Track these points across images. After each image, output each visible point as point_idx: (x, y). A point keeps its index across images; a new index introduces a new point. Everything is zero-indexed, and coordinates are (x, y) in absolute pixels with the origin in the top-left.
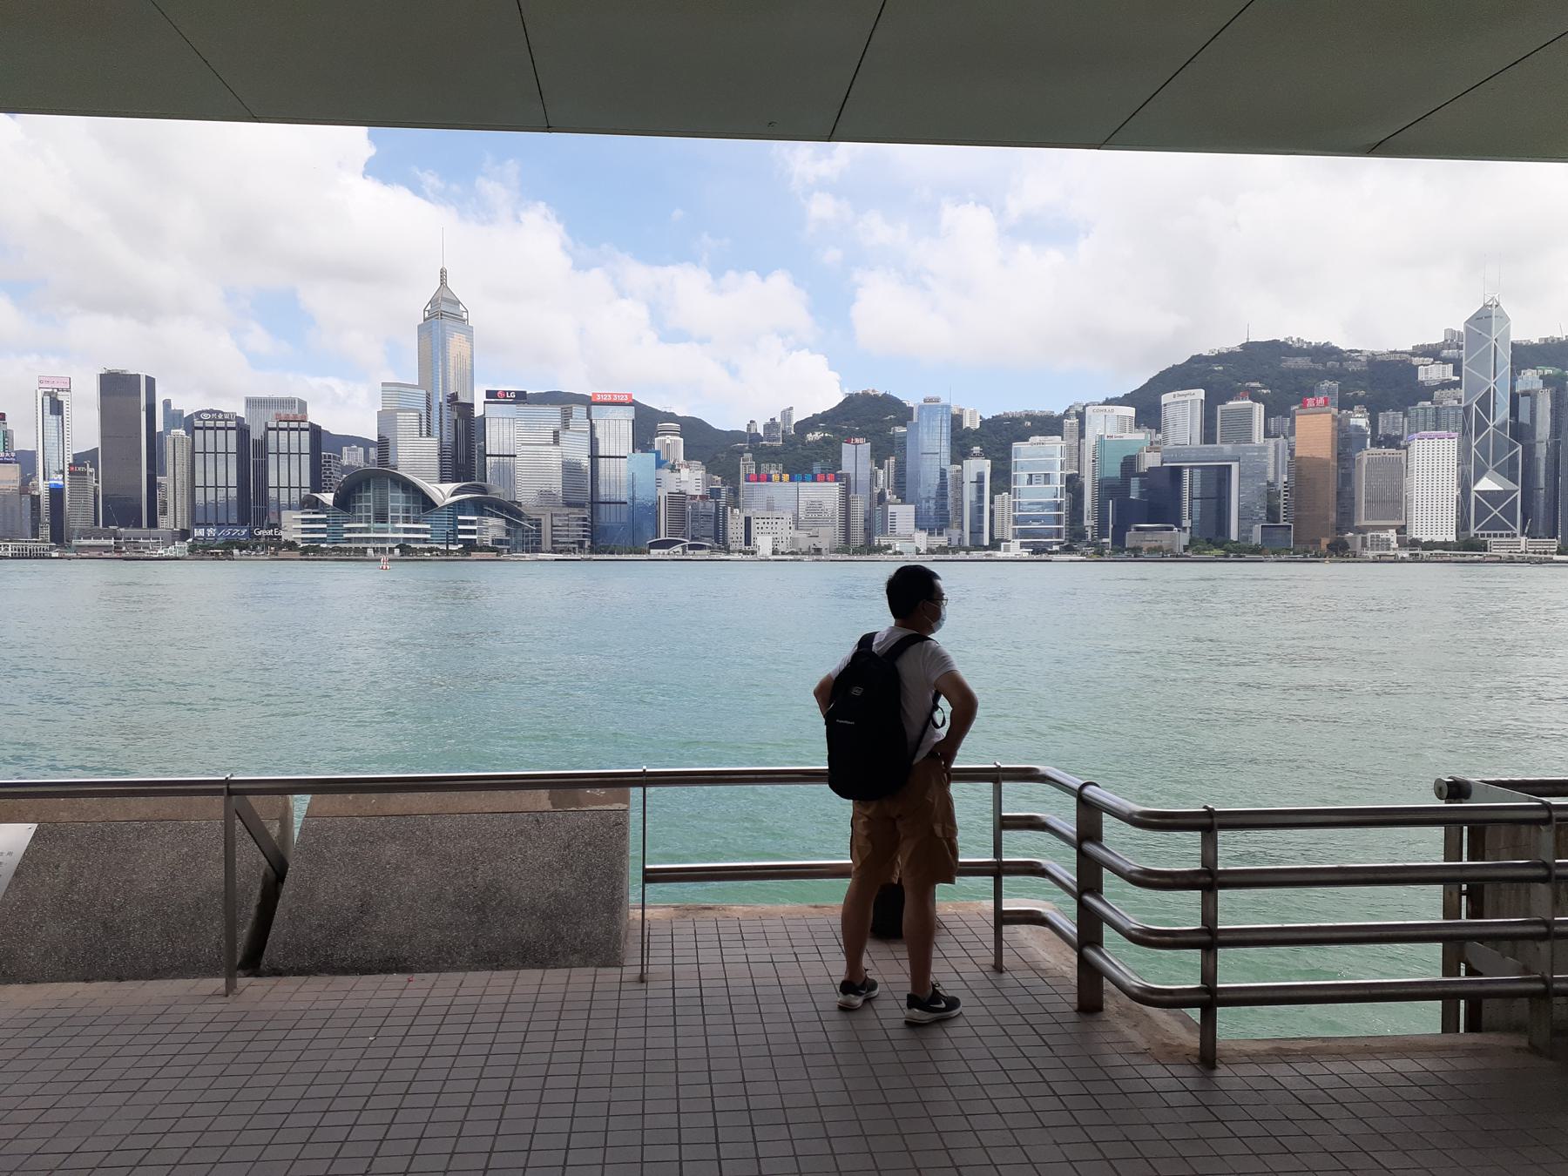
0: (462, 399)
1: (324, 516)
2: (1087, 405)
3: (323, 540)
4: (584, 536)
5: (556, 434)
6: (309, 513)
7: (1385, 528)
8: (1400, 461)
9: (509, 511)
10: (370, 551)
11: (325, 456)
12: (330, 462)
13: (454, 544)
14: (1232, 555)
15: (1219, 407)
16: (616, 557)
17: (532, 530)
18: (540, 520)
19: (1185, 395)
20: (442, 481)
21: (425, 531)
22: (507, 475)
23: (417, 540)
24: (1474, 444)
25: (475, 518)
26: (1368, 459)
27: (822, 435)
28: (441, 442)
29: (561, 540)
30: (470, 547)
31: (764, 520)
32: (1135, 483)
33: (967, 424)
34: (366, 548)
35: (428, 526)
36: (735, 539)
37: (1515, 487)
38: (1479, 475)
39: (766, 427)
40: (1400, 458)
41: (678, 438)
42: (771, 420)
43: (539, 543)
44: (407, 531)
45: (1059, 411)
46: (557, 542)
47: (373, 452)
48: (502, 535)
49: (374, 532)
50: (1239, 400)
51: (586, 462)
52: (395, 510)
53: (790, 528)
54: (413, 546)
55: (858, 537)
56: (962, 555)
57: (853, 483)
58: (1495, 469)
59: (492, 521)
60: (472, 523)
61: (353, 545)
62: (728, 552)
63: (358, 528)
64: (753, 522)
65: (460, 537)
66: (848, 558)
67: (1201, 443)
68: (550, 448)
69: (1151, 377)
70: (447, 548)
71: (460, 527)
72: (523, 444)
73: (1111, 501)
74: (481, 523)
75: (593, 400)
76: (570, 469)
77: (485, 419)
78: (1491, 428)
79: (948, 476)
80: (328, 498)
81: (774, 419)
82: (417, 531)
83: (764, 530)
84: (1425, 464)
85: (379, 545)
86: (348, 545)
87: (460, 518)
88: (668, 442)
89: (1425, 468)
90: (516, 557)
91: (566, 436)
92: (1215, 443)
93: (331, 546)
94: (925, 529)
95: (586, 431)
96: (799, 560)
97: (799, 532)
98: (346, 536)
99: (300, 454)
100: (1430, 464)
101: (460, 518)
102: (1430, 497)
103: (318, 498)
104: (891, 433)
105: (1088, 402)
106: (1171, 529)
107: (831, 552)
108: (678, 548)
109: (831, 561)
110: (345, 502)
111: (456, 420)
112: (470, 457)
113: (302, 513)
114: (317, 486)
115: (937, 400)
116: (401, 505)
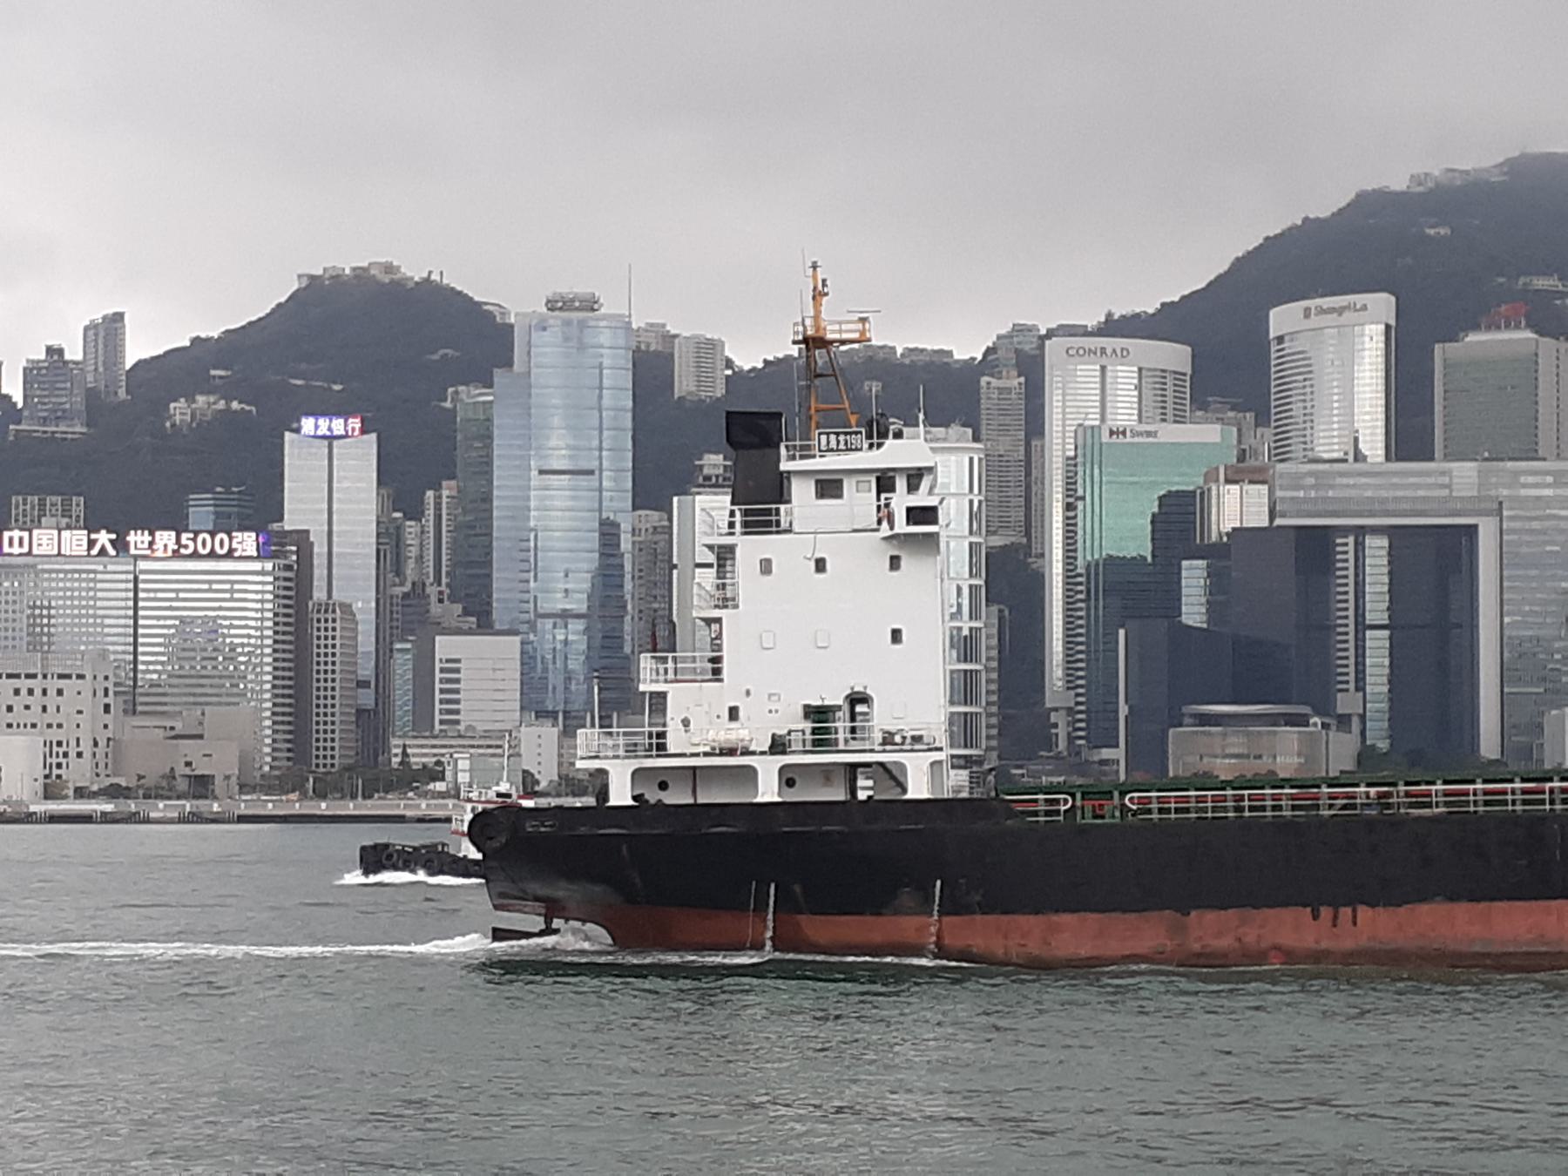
2: (1051, 334)
15: (1438, 347)
19: (1340, 311)
32: (1193, 575)
33: (684, 384)
39: (32, 374)
42: (50, 350)
45: (967, 348)
50: (1498, 328)
53: (107, 708)
57: (319, 562)
67: (1388, 458)
73: (1122, 632)
79: (626, 543)
92: (1431, 459)
94: (553, 715)
96: (132, 818)
104: (448, 405)
105: (1054, 326)
107: (243, 788)
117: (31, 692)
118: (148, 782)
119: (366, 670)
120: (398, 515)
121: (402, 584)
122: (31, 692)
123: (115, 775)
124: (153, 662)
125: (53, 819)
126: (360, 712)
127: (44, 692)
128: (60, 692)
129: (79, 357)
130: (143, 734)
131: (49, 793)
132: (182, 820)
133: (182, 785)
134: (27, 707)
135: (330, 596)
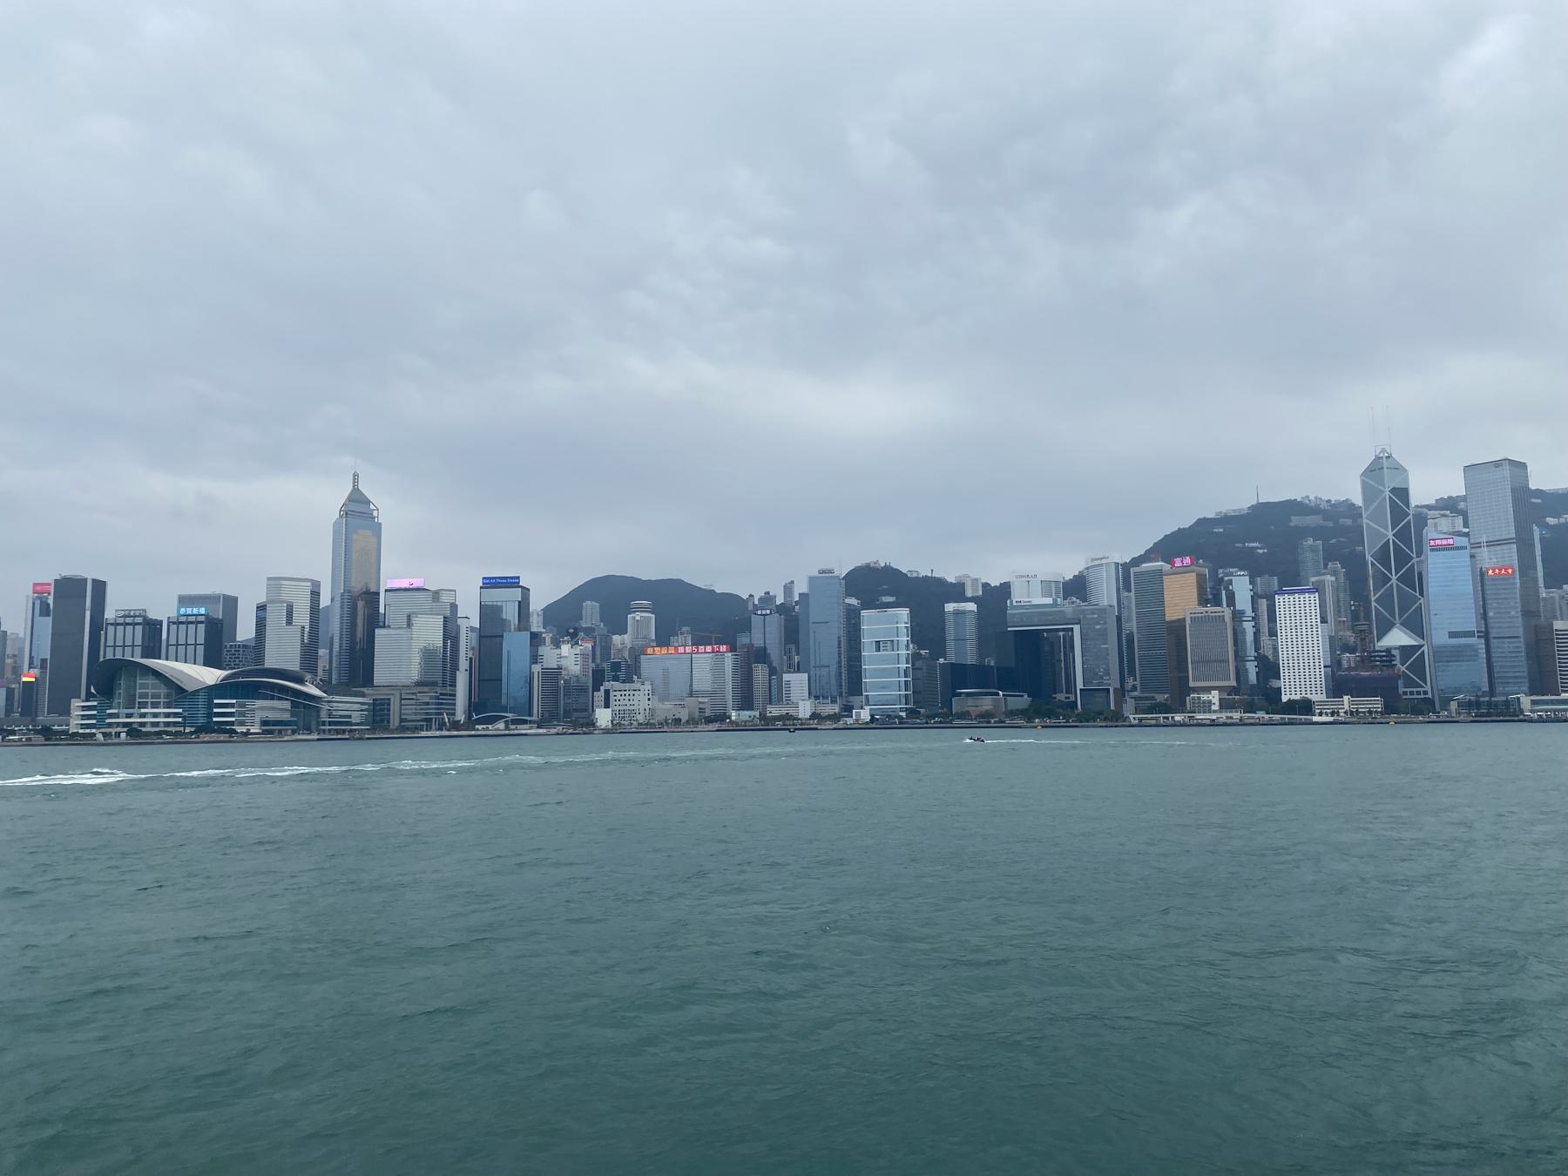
0: (373, 589)
7: (1208, 690)
8: (1224, 619)
10: (100, 737)
14: (993, 721)
18: (389, 699)
24: (1373, 599)
26: (1191, 618)
34: (94, 734)
37: (1422, 642)
38: (1385, 628)
40: (1223, 616)
41: (650, 615)
56: (666, 729)
58: (1401, 624)
63: (119, 715)
68: (401, 631)
69: (1156, 541)
71: (215, 710)
74: (243, 706)
78: (1394, 578)
81: (768, 593)
84: (1288, 622)
87: (216, 701)
89: (1288, 624)
99: (133, 646)
100: (1293, 621)
101: (216, 701)
102: (1316, 655)
106: (1023, 696)
108: (501, 725)
115: (831, 572)
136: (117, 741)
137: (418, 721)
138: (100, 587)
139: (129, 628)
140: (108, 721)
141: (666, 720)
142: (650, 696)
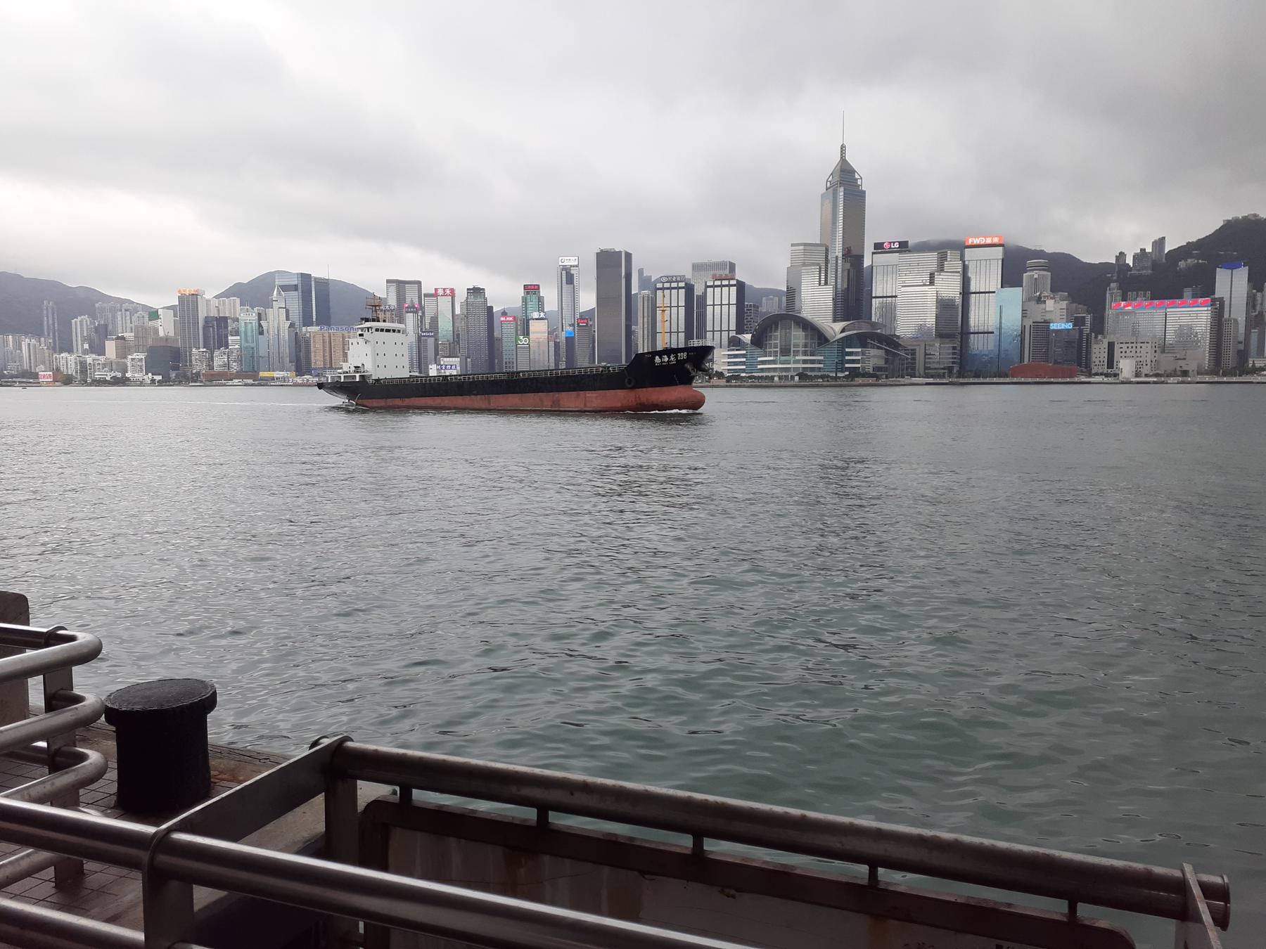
1: (744, 352)
3: (743, 371)
4: (953, 363)
5: (932, 276)
6: (733, 350)
9: (889, 342)
10: (776, 379)
11: (747, 305)
12: (751, 310)
13: (842, 372)
16: (981, 380)
17: (907, 359)
20: (835, 321)
21: (819, 362)
22: (890, 312)
23: (812, 369)
25: (860, 350)
27: (1196, 261)
28: (836, 288)
29: (933, 366)
30: (854, 373)
31: (1127, 345)
35: (822, 358)
36: (1097, 363)
41: (1045, 273)
43: (914, 369)
44: (805, 362)
46: (929, 368)
47: (784, 299)
48: (881, 363)
49: (780, 363)
51: (958, 300)
52: (796, 345)
53: (1155, 351)
54: (809, 374)
55: (1230, 360)
59: (873, 352)
60: (856, 354)
61: (764, 374)
62: (1090, 375)
64: (1117, 347)
65: (847, 365)
66: (1216, 379)
70: (836, 374)
71: (847, 358)
72: (903, 286)
75: (967, 244)
76: (944, 306)
77: (872, 267)
80: (747, 337)
82: (813, 362)
83: (1128, 354)
85: (784, 374)
86: (760, 374)
87: (847, 350)
88: (1036, 276)
90: (893, 381)
91: (940, 277)
93: (747, 375)
95: (958, 272)
96: (1162, 383)
97: (1165, 355)
98: (759, 367)
101: (847, 350)
103: (740, 339)
107: (1198, 374)
109: (1198, 383)
110: (759, 342)
111: (849, 270)
112: (858, 301)
113: (729, 350)
114: (740, 329)
116: (801, 341)
117: (1132, 347)
118: (1169, 372)
119: (1241, 338)
120: (1255, 291)
121: (1255, 312)
122: (1132, 347)
123: (1158, 369)
124: (1170, 337)
125: (1138, 383)
126: (1239, 352)
127: (1136, 347)
128: (1141, 347)
129: (1151, 251)
130: (1168, 357)
131: (1137, 375)
132: (1178, 383)
133: (1179, 373)
134: (1131, 352)
135: (1230, 316)
136: (792, 383)
137: (943, 369)
138: (628, 256)
139: (674, 292)
140: (759, 367)
141: (1175, 370)
142: (1157, 349)
